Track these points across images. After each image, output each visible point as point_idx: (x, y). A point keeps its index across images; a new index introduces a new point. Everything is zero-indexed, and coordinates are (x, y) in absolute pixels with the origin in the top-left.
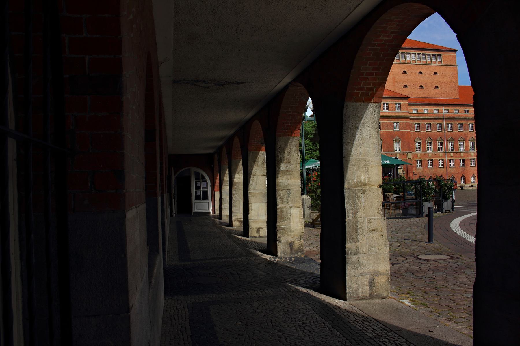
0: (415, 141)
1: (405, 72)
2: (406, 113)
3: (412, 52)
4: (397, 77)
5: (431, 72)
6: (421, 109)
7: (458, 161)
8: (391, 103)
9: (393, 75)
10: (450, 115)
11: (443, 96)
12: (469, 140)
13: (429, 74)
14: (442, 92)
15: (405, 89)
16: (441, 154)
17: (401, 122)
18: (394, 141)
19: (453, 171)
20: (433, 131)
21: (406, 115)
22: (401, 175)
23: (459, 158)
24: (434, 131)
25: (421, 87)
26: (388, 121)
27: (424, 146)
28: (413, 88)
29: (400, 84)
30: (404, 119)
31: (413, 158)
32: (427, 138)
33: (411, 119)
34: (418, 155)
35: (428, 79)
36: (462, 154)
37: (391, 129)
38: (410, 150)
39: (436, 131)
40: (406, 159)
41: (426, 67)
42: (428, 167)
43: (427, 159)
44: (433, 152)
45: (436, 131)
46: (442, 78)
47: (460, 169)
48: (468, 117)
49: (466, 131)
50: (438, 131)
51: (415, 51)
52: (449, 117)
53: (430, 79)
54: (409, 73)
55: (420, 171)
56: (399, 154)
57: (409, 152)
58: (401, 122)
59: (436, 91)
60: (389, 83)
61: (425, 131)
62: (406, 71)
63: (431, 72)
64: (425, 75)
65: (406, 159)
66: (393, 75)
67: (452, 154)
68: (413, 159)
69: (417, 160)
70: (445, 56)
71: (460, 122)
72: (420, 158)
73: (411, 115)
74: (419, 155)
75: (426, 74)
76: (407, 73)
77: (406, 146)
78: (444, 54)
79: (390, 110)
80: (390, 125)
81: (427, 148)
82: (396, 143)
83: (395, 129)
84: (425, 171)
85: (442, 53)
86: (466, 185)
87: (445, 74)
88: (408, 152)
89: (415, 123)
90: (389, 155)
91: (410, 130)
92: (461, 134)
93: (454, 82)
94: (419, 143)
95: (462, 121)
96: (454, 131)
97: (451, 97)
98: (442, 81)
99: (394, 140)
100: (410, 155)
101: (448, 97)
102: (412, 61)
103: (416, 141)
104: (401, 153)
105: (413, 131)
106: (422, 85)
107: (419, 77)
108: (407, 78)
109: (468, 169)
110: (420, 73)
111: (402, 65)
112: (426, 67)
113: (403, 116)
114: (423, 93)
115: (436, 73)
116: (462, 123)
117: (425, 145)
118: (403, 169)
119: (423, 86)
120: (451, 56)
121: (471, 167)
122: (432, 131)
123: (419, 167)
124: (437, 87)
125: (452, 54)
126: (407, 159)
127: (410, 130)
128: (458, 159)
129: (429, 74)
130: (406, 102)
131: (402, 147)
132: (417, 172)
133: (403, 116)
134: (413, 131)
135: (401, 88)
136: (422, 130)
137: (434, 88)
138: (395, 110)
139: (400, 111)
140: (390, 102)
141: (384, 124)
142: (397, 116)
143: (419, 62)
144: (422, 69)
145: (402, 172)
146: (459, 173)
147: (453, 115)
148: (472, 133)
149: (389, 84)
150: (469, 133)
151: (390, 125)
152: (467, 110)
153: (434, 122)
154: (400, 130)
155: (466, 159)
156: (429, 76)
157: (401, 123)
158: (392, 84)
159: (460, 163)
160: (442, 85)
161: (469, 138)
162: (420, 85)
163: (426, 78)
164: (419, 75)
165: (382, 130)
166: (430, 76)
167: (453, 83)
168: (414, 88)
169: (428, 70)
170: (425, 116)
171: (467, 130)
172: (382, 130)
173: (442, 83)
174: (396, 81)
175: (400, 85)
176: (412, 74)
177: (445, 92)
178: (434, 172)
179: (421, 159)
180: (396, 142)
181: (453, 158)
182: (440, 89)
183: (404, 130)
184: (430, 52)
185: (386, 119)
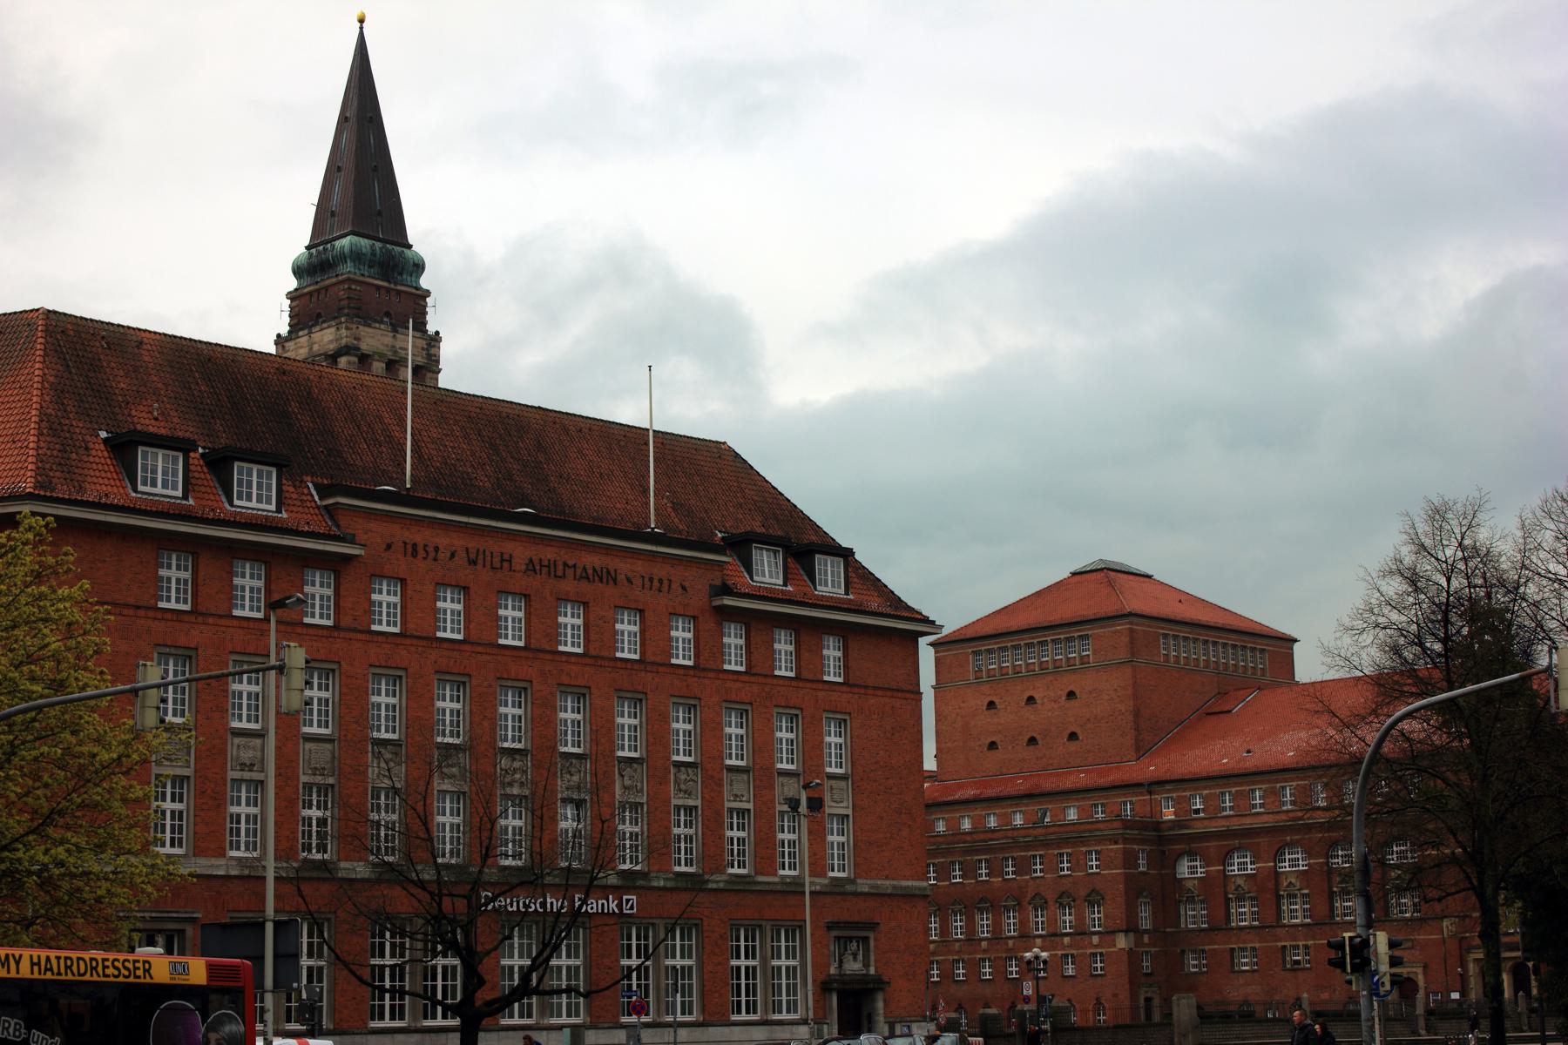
3: (1012, 641)
5: (1059, 693)
9: (962, 717)
23: (1004, 955)
28: (1010, 747)
35: (1050, 714)
36: (1011, 942)
54: (1003, 706)
63: (1059, 693)
64: (1043, 704)
75: (1045, 700)
85: (1089, 629)
108: (996, 720)
110: (1031, 700)
119: (1038, 738)
120: (1115, 632)
128: (1000, 958)
156: (1053, 704)
171: (1026, 874)
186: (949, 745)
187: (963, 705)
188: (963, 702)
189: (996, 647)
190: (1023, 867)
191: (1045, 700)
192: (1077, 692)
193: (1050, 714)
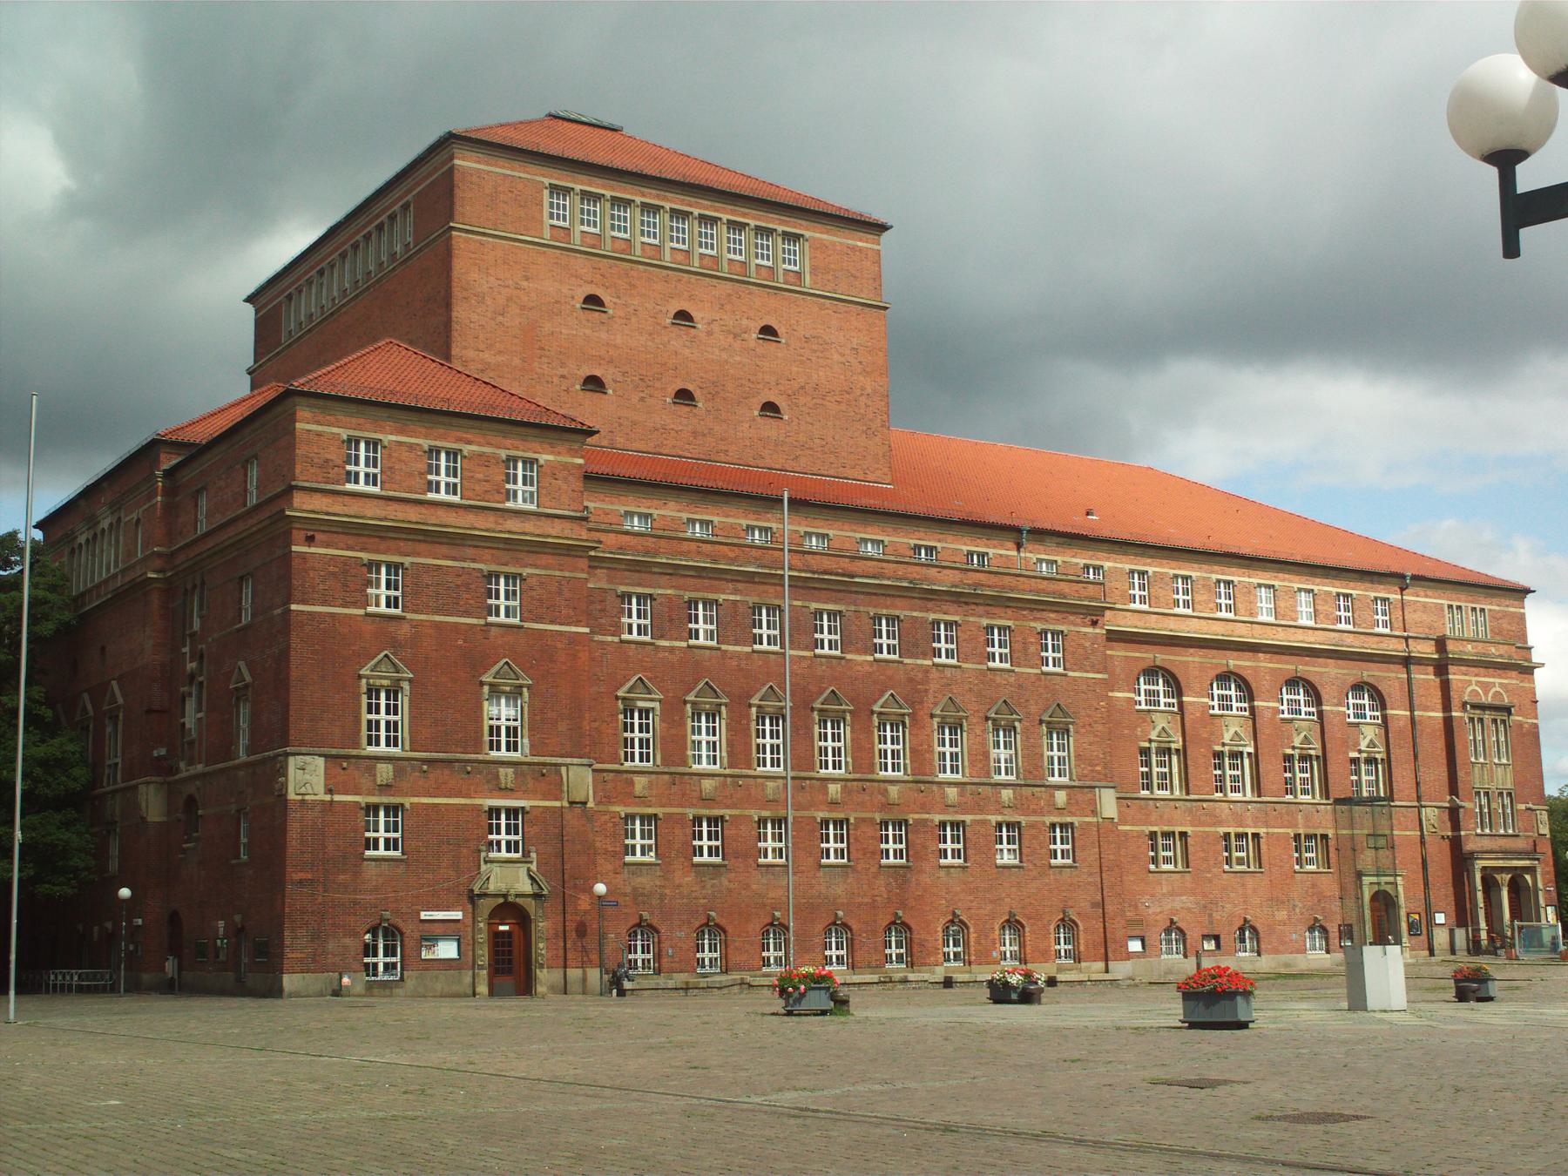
0: (617, 698)
1: (593, 301)
2: (567, 525)
4: (548, 327)
5: (745, 322)
6: (673, 519)
7: (870, 831)
8: (481, 455)
10: (828, 563)
11: (803, 463)
12: (932, 716)
13: (729, 332)
14: (802, 437)
15: (591, 398)
16: (770, 784)
17: (537, 571)
18: (486, 689)
19: (839, 891)
20: (731, 648)
21: (567, 533)
22: (519, 901)
23: (878, 817)
24: (738, 648)
25: (684, 396)
26: (454, 559)
27: (673, 731)
28: (635, 399)
29: (563, 365)
30: (550, 560)
31: (605, 798)
32: (696, 682)
33: (596, 563)
34: (632, 783)
35: (724, 356)
37: (467, 614)
38: (583, 746)
39: (748, 649)
40: (557, 804)
41: (716, 293)
42: (697, 859)
43: (691, 813)
44: (728, 771)
45: (748, 649)
46: (802, 362)
47: (881, 881)
48: (926, 579)
49: (919, 662)
50: (757, 647)
51: (658, 197)
52: (825, 572)
53: (738, 358)
54: (621, 313)
55: (644, 881)
56: (510, 771)
57: (575, 761)
58: (537, 571)
59: (769, 428)
60: (500, 352)
61: (684, 644)
62: (606, 298)
63: (745, 322)
64: (709, 333)
65: (557, 804)
66: (523, 308)
67: (834, 789)
68: (601, 808)
69: (631, 818)
70: (818, 247)
71: (887, 607)
72: (642, 800)
73: (602, 536)
74: (640, 783)
75: (716, 327)
76: (611, 312)
77: (563, 727)
78: (818, 235)
79: (471, 494)
80: (467, 585)
81: (689, 744)
82: (499, 704)
83: (498, 615)
84: (677, 882)
86: (911, 977)
87: (821, 341)
88: (568, 760)
89: (622, 589)
90: (446, 772)
91: (587, 630)
92: (890, 678)
93: (869, 391)
94: (647, 711)
95: (898, 602)
96: (849, 656)
97: (849, 472)
98: (802, 381)
99: (482, 684)
100: (580, 779)
101: (831, 472)
102: (643, 250)
103: (624, 699)
104: (525, 767)
105: (609, 639)
106: (690, 388)
107: (677, 340)
108: (604, 336)
109: (926, 879)
110: (683, 316)
111: (580, 264)
112: (716, 293)
113: (548, 536)
114: (694, 433)
115: (768, 331)
116: (897, 613)
117: (684, 725)
118: (534, 867)
119: (697, 394)
120: (854, 248)
121: (942, 873)
122: (724, 647)
123: (638, 857)
124: (770, 408)
125: (861, 240)
126: (566, 804)
127: (587, 630)
129: (729, 332)
130: (574, 453)
131: (538, 722)
132: (628, 890)
133: (548, 536)
134: (609, 639)
135: (567, 391)
136: (662, 637)
137: (756, 413)
138: (497, 497)
139: (533, 507)
140: (474, 448)
141: (427, 579)
142: (510, 532)
143: (680, 257)
144: (691, 298)
145: (526, 887)
146: (873, 906)
147: (845, 564)
148: (948, 672)
149: (500, 358)
150: (934, 674)
151: (467, 585)
152: (926, 548)
153: (735, 592)
154: (526, 625)
155: (917, 821)
157: (533, 582)
158: (517, 361)
159: (883, 846)
160: (802, 400)
161: (931, 698)
162: (680, 385)
163: (717, 351)
164: (675, 329)
165: (409, 616)
166: (737, 345)
167: (863, 399)
168: (642, 399)
169: (728, 307)
170: (685, 554)
171: (924, 656)
172: (409, 616)
173: (802, 388)
174: (542, 349)
175: (564, 371)
176: (634, 320)
177: (817, 441)
178: (730, 891)
179: (650, 811)
180: (496, 691)
181: (841, 816)
182: (790, 421)
183: (552, 622)
184: (744, 215)
185: (444, 549)
186: (486, 356)
187: (525, 284)
188: (527, 279)
189: (608, 194)
190: (916, 641)
191: (716, 327)
192: (781, 330)
193: (724, 356)
